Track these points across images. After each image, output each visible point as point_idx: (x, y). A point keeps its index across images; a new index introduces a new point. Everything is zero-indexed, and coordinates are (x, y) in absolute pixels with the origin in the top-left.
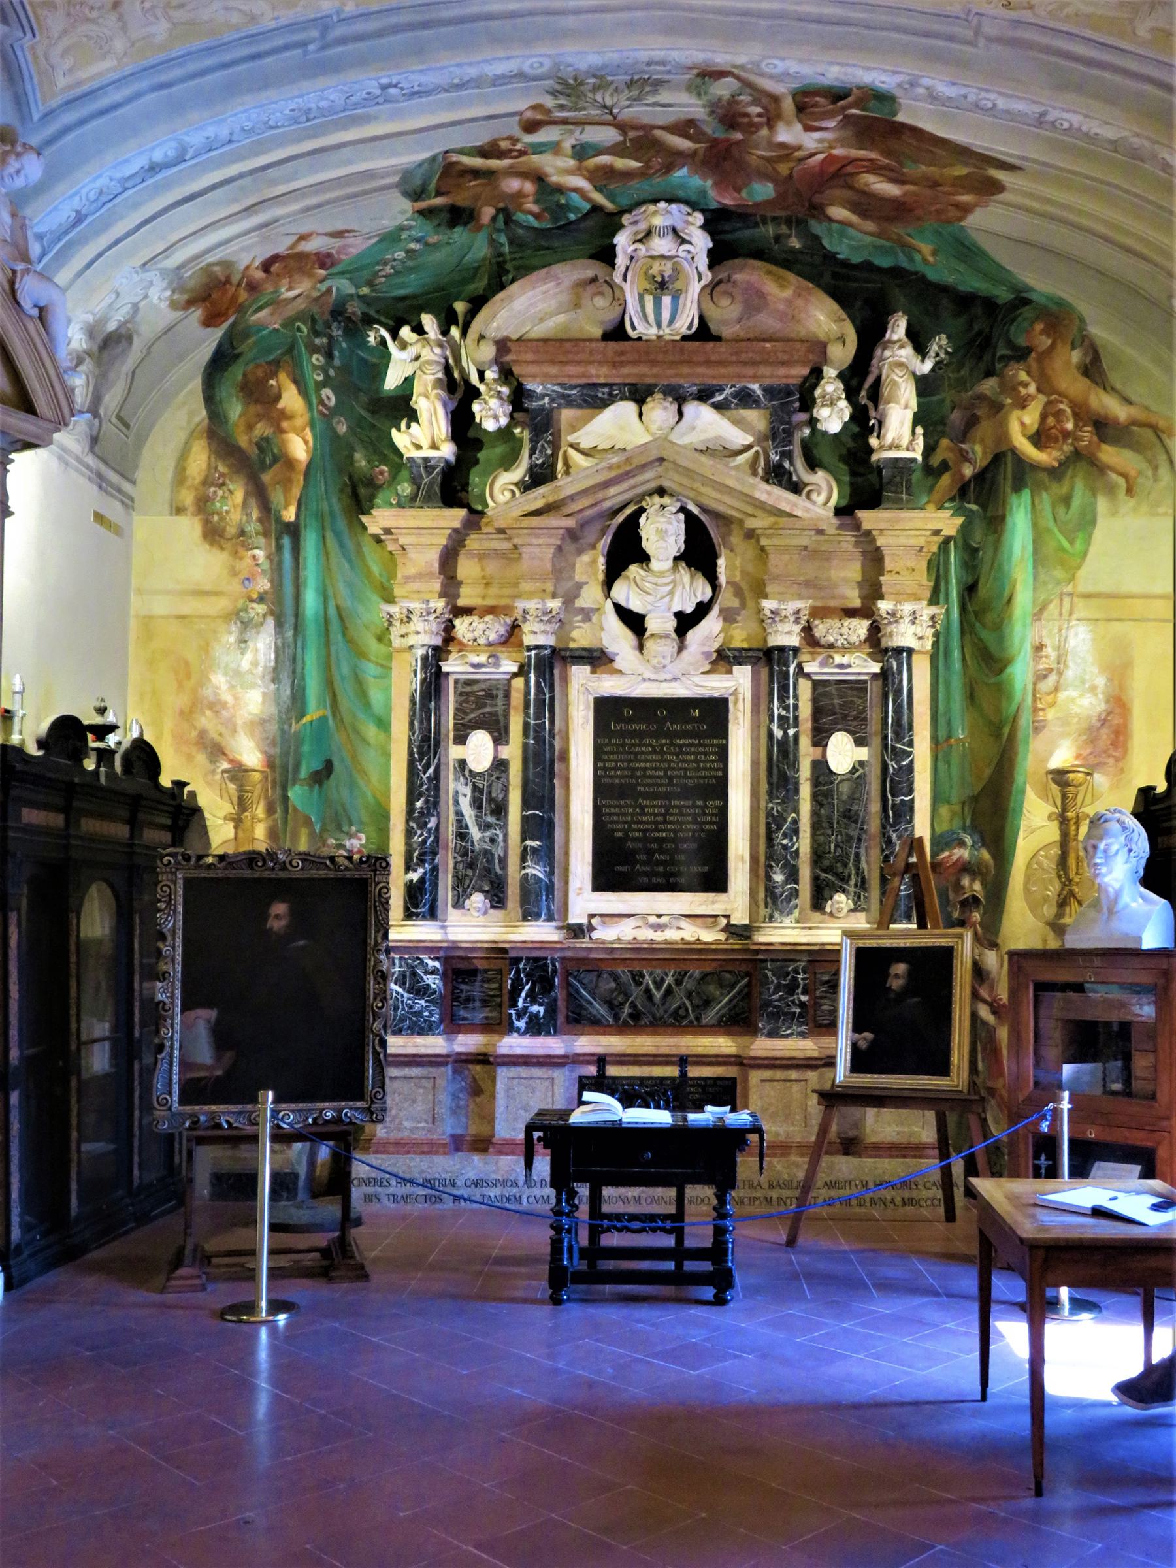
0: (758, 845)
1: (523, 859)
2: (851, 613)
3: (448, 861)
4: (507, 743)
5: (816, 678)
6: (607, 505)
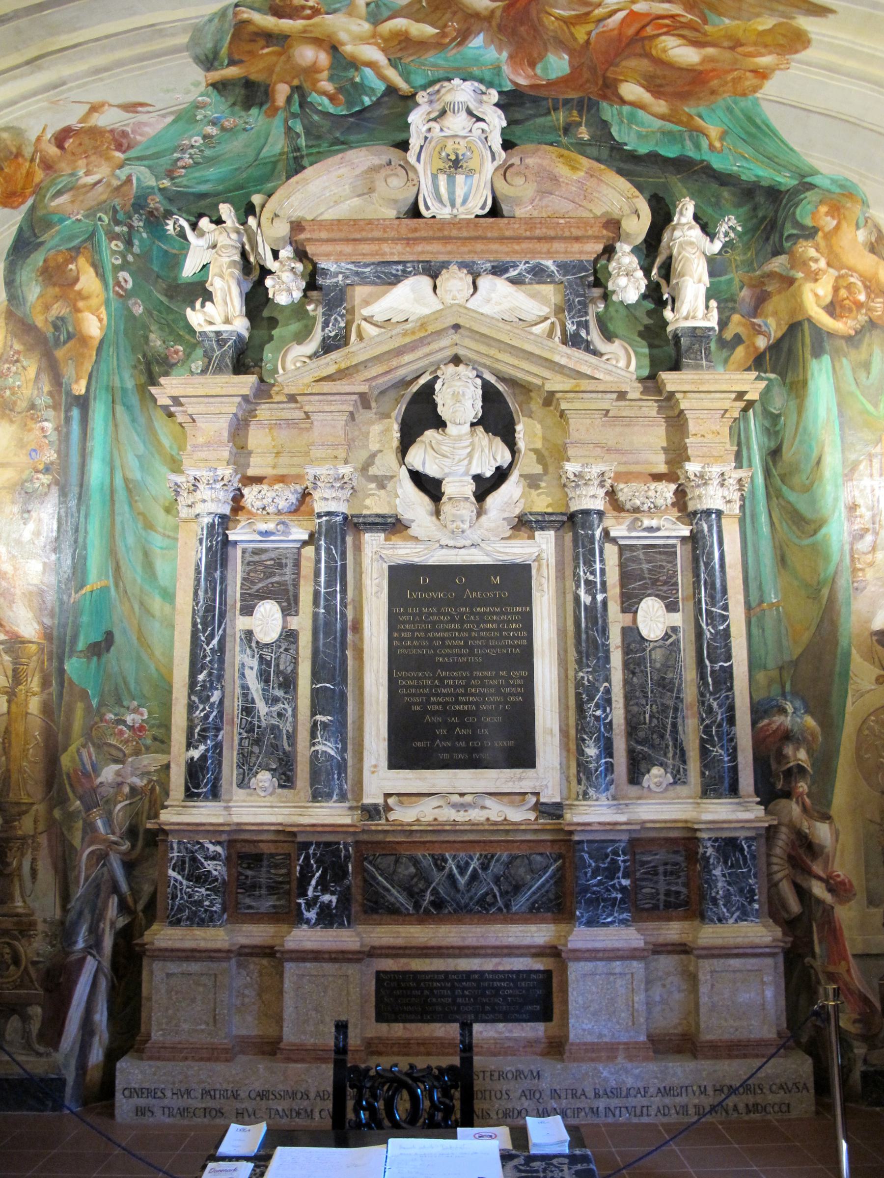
0: (567, 718)
1: (313, 735)
2: (657, 477)
3: (231, 738)
4: (297, 614)
5: (621, 542)
6: (401, 373)
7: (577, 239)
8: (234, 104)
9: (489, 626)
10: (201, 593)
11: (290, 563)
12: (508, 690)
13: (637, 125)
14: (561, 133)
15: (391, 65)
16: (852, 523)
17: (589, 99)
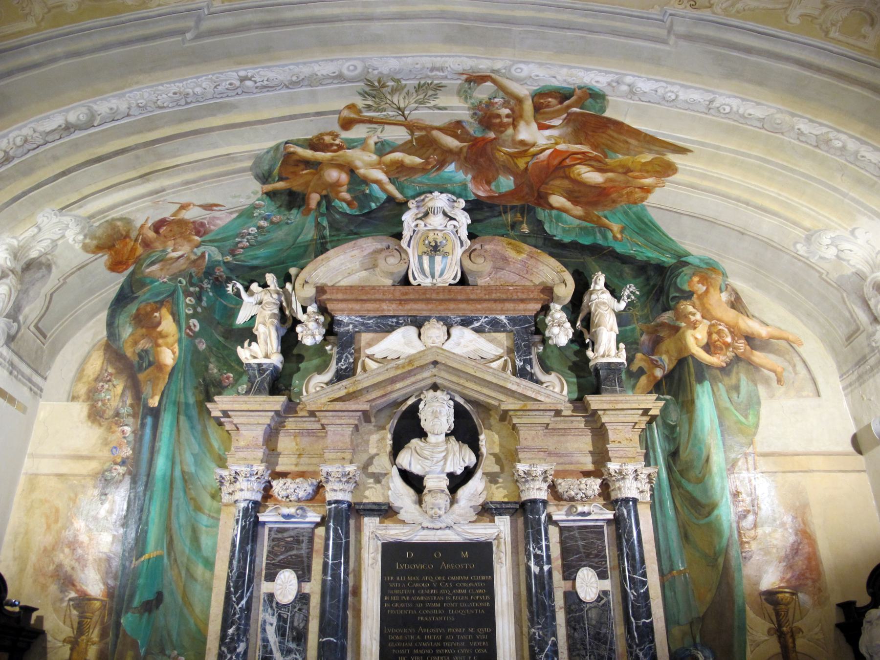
2: (587, 474)
4: (309, 580)
5: (562, 524)
6: (394, 396)
7: (522, 301)
8: (280, 206)
9: (460, 591)
10: (235, 563)
11: (306, 539)
12: (475, 644)
16: (737, 506)
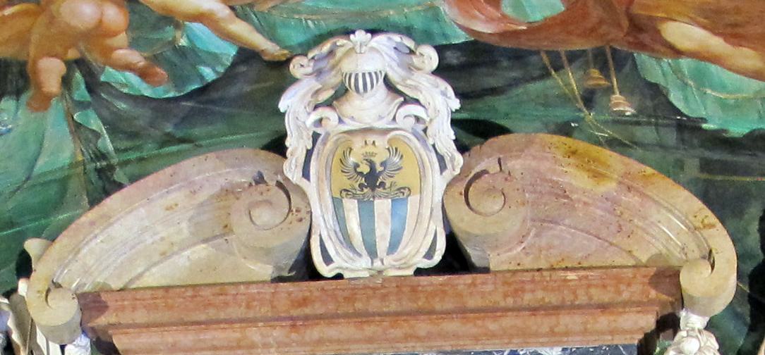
7: (604, 307)
13: (713, 89)
14: (580, 104)
15: (237, 16)
17: (614, 51)
